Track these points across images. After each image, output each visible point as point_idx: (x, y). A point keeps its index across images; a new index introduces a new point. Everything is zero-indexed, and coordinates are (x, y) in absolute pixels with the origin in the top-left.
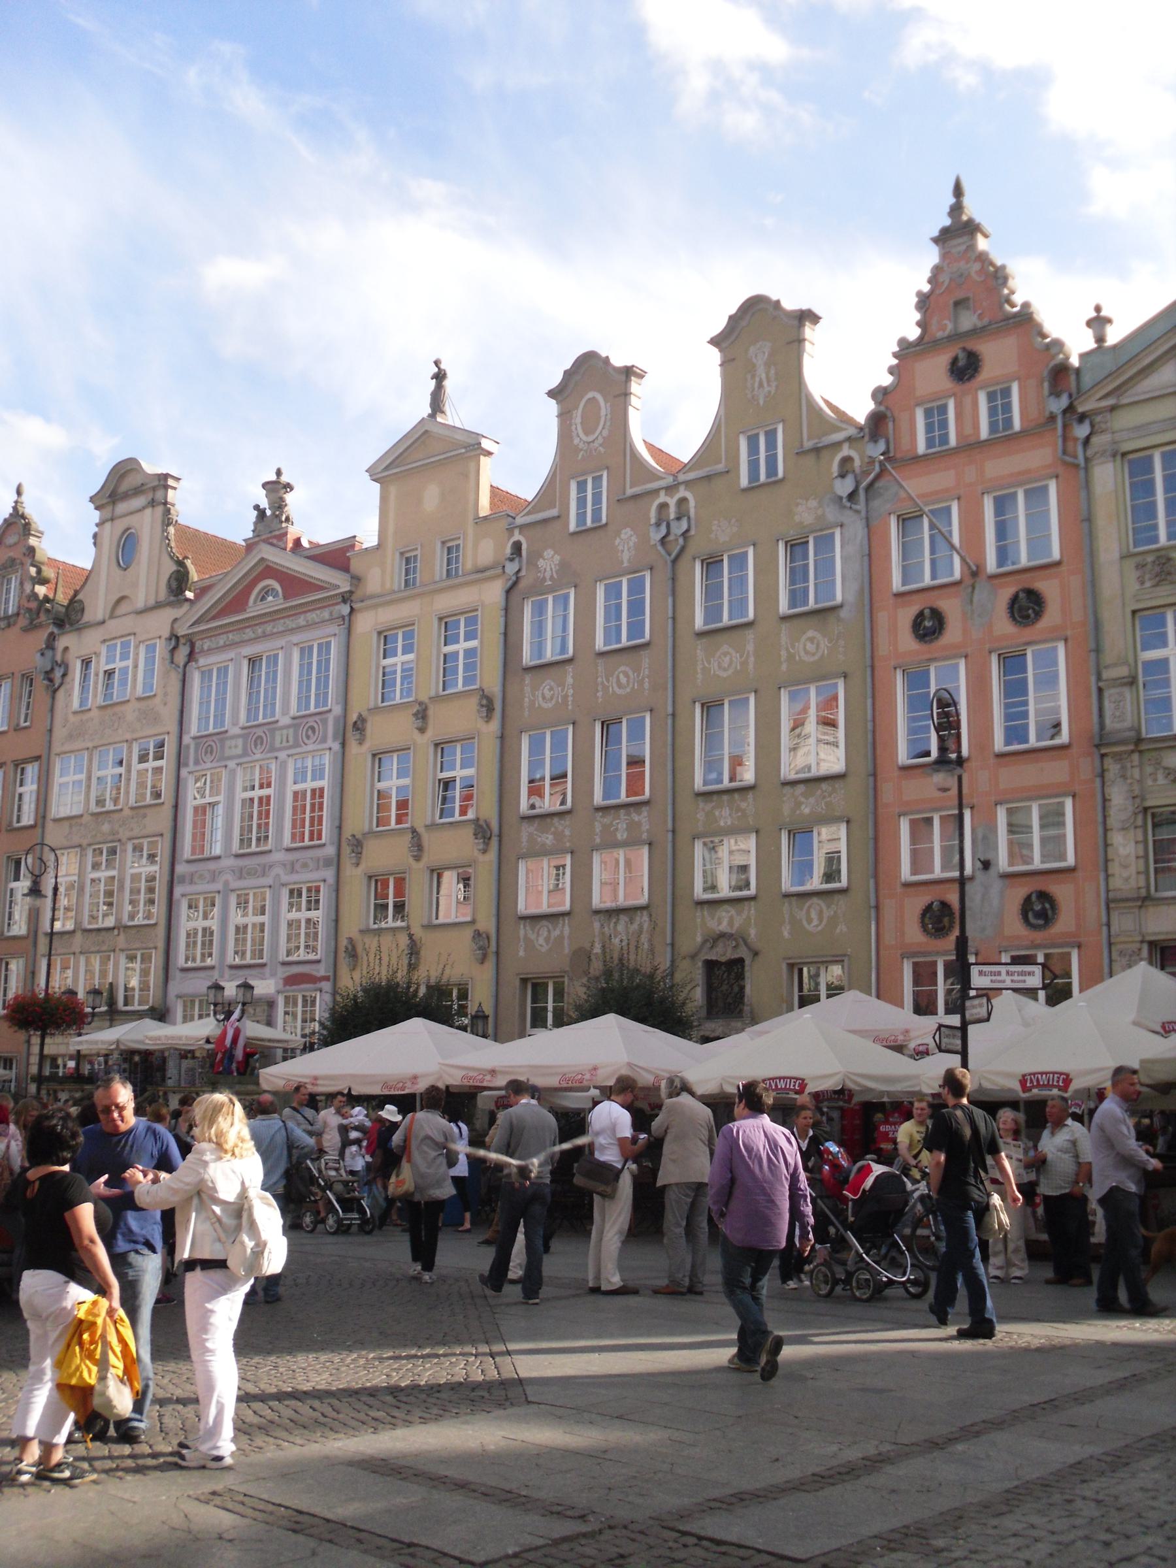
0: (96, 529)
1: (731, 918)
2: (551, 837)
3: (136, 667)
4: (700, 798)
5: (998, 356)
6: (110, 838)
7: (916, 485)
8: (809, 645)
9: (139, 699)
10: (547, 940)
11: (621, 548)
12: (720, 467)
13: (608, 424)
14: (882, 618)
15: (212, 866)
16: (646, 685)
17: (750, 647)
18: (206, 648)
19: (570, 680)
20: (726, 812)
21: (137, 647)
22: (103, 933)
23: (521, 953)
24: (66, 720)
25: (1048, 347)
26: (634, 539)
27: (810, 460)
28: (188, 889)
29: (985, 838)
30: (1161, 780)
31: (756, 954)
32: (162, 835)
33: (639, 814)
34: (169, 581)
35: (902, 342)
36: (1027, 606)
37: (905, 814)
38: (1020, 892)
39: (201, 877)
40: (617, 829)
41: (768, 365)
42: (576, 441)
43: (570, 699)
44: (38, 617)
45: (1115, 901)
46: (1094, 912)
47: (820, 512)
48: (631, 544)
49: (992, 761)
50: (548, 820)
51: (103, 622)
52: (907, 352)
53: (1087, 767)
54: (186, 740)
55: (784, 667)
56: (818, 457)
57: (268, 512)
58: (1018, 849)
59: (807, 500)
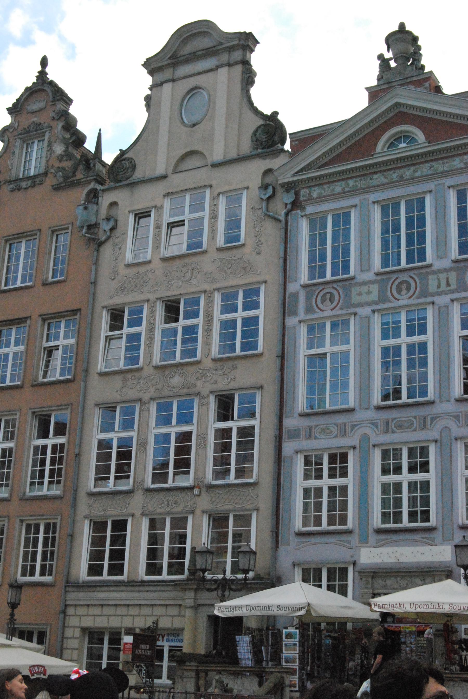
0: (149, 92)
3: (214, 217)
6: (185, 391)
9: (220, 250)
15: (341, 419)
18: (315, 195)
21: (214, 199)
22: (175, 493)
24: (116, 272)
28: (305, 444)
32: (261, 387)
34: (256, 131)
39: (325, 431)
44: (74, 174)
51: (164, 177)
54: (292, 288)
57: (393, 64)
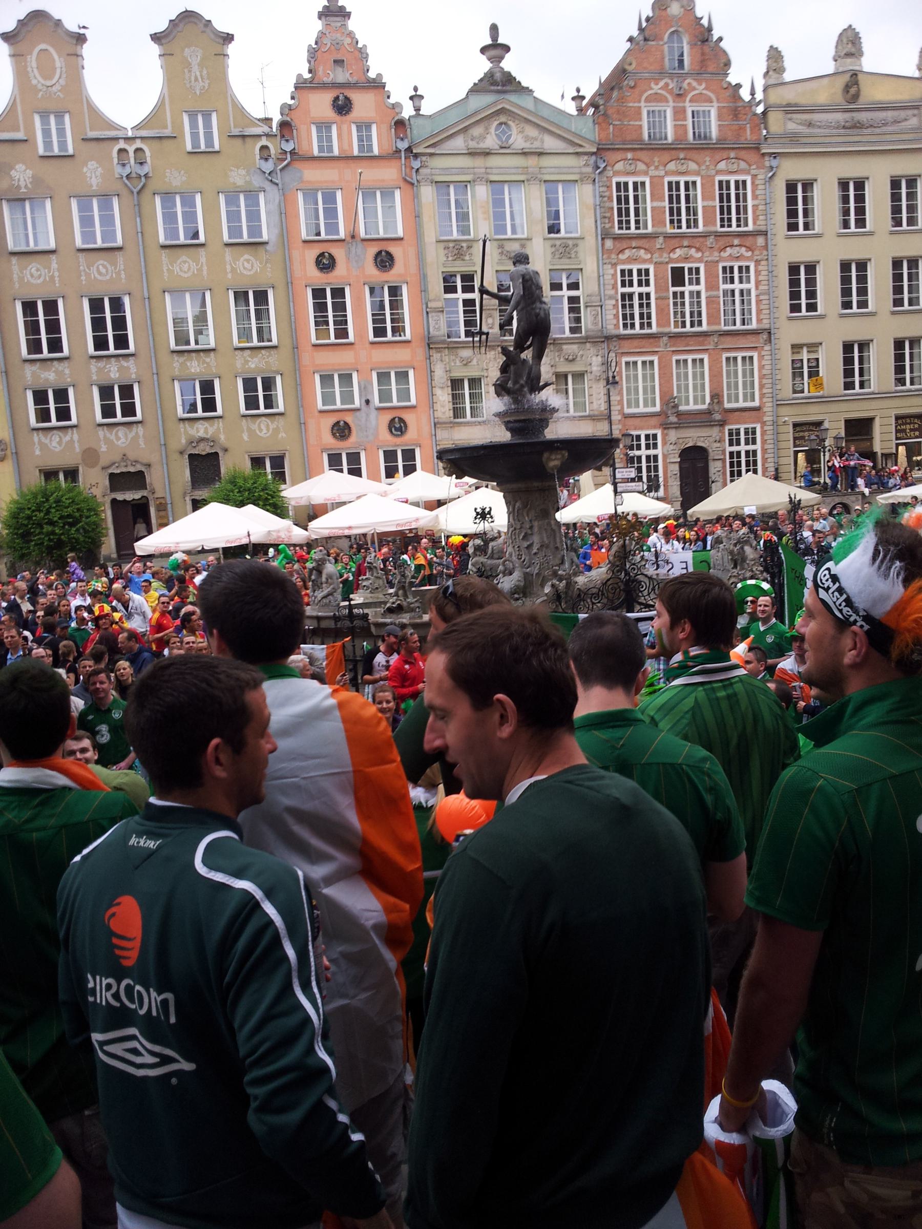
1: (206, 428)
2: (53, 374)
4: (175, 355)
5: (363, 103)
7: (312, 174)
8: (246, 264)
10: (60, 443)
11: (88, 175)
12: (167, 132)
13: (64, 76)
14: (296, 254)
16: (123, 276)
17: (203, 260)
19: (54, 265)
20: (195, 363)
23: (38, 452)
25: (394, 106)
26: (99, 169)
27: (239, 142)
29: (365, 388)
30: (458, 363)
31: (226, 450)
33: (127, 362)
35: (299, 76)
36: (384, 260)
37: (317, 372)
38: (388, 417)
40: (110, 371)
41: (201, 65)
42: (34, 82)
43: (57, 279)
45: (438, 423)
46: (426, 429)
47: (248, 178)
48: (98, 173)
49: (368, 345)
50: (49, 363)
52: (301, 86)
53: (420, 352)
55: (230, 276)
56: (244, 142)
58: (385, 396)
59: (238, 168)
